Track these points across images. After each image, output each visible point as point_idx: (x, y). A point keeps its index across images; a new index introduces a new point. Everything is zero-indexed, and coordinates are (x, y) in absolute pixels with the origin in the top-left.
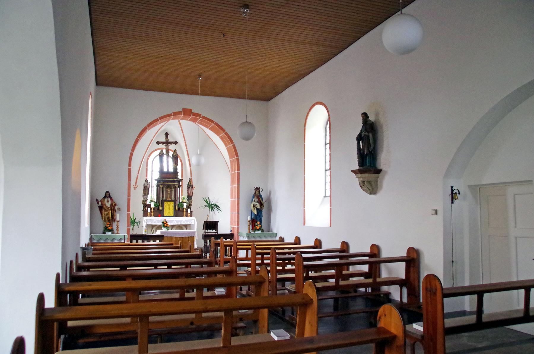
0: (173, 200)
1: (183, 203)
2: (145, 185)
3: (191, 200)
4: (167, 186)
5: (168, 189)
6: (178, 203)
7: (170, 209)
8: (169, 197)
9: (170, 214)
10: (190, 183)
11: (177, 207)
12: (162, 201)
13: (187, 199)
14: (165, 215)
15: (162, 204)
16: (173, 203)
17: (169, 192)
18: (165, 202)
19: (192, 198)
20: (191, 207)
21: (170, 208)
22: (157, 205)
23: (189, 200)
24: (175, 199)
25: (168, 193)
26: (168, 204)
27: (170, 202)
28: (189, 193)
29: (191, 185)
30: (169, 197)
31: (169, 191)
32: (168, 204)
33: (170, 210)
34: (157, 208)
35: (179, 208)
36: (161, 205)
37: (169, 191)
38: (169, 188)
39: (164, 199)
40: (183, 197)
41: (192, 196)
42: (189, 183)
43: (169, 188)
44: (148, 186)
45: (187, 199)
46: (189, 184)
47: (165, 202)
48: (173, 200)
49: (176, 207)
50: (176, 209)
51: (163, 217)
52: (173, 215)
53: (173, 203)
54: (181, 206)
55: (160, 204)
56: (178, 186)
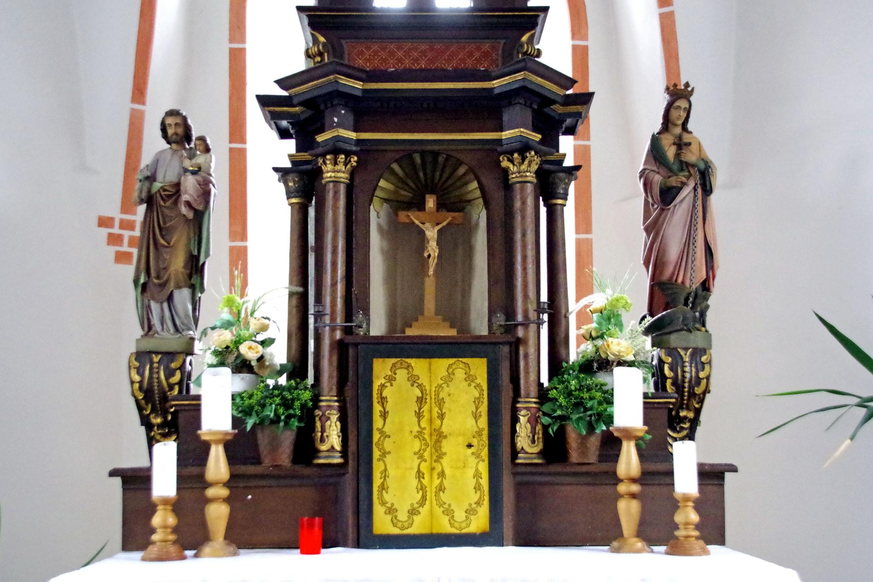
0: (485, 332)
1: (601, 378)
2: (160, 176)
3: (696, 339)
4: (401, 182)
5: (421, 206)
6: (544, 379)
7: (439, 456)
8: (430, 305)
9: (449, 512)
10: (681, 145)
11: (534, 421)
12: (341, 348)
13: (648, 331)
14: (382, 524)
15: (341, 393)
16: (479, 367)
17: (433, 249)
18: (381, 368)
19: (703, 315)
20: (695, 422)
21: (439, 436)
22: (287, 404)
23: (674, 340)
24: (500, 319)
25: (423, 262)
26: (413, 380)
27: (441, 365)
28: (673, 251)
29: (690, 157)
30: (430, 305)
31: (432, 233)
32: (413, 380)
33: (445, 461)
34: (287, 438)
35: (562, 432)
36: (329, 400)
37: (432, 233)
38: (431, 202)
39: (378, 326)
40: (598, 300)
41: (706, 286)
42: (667, 141)
43: (431, 202)
44: (190, 183)
45: (648, 331)
46: (671, 152)
47: (381, 368)
48: (485, 332)
49: (523, 428)
50: (522, 442)
51: (358, 545)
52: (479, 522)
53: (479, 367)
54: (579, 404)
55: (316, 399)
56: (533, 162)
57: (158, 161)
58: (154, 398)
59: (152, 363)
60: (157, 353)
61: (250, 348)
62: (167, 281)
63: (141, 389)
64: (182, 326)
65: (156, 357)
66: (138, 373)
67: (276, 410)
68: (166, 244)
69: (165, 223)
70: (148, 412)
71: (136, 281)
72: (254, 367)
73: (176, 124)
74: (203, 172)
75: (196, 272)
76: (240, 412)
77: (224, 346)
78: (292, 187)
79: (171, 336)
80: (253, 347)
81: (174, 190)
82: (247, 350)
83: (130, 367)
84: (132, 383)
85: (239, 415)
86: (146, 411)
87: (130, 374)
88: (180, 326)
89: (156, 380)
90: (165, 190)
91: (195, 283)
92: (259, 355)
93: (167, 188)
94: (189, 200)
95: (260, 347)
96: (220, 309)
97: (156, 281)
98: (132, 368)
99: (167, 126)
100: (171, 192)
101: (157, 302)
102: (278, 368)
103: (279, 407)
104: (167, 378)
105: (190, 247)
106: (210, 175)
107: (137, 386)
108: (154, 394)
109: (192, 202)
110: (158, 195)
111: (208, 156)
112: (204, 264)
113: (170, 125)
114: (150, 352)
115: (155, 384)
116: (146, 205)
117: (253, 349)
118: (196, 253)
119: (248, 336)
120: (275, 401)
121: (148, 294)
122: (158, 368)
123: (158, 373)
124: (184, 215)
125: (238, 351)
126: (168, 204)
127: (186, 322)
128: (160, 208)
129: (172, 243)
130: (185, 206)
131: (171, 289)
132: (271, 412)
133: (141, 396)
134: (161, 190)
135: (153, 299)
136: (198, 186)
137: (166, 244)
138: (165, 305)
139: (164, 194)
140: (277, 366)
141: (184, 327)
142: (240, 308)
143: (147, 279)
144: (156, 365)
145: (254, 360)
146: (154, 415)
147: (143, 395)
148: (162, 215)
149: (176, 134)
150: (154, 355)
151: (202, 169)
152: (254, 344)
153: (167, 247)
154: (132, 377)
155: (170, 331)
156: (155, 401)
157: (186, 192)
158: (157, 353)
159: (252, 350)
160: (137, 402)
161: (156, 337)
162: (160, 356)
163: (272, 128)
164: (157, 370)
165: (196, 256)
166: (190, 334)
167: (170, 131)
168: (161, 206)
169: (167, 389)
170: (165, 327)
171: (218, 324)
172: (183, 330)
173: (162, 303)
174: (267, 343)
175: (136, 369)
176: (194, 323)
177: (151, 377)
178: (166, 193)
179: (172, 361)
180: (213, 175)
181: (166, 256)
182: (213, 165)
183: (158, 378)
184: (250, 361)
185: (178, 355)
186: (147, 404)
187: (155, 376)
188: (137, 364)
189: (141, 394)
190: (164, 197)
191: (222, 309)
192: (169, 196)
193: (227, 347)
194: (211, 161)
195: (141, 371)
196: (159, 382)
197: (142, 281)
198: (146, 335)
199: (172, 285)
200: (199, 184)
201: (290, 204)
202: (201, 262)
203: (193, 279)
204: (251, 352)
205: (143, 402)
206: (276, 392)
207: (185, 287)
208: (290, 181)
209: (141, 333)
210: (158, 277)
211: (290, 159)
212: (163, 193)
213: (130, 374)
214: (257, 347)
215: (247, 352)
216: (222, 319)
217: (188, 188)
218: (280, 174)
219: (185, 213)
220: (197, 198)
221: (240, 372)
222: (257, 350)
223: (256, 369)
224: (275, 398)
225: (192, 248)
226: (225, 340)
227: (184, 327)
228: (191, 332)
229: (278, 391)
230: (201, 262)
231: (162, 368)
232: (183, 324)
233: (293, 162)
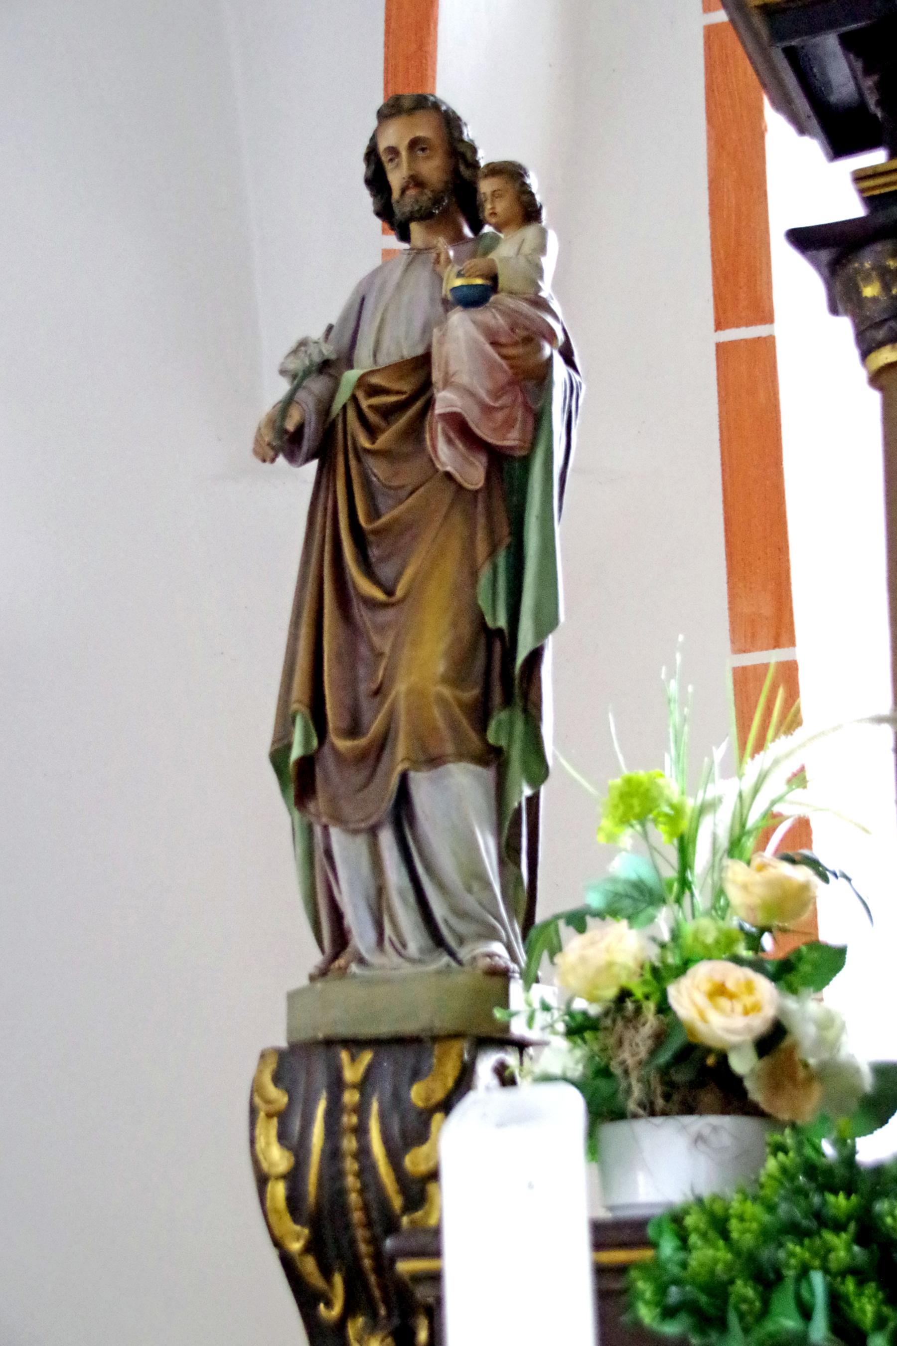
57: (363, 300)
58: (353, 1242)
59: (337, 1085)
60: (355, 1044)
61: (719, 991)
62: (383, 743)
63: (294, 1202)
64: (453, 921)
65: (353, 1059)
66: (282, 1137)
67: (836, 1302)
68: (379, 595)
69: (374, 513)
70: (336, 1311)
71: (279, 758)
72: (749, 1084)
73: (415, 144)
74: (511, 293)
75: (508, 701)
76: (668, 1313)
77: (611, 993)
78: (874, 299)
79: (407, 969)
80: (730, 985)
81: (407, 386)
82: (702, 1000)
83: (253, 1112)
84: (262, 1180)
85: (671, 1329)
86: (329, 1305)
87: (252, 1141)
88: (446, 921)
89: (351, 1165)
90: (374, 391)
91: (503, 743)
92: (759, 1023)
93: (375, 380)
94: (458, 410)
95: (764, 987)
96: (601, 839)
97: (343, 744)
98: (262, 1114)
99: (384, 158)
100: (398, 393)
101: (355, 832)
102: (868, 1082)
103: (850, 1285)
104: (395, 1158)
105: (474, 598)
106: (542, 305)
107: (278, 1191)
108: (348, 1226)
109: (473, 417)
110: (351, 414)
111: (530, 232)
112: (536, 656)
113: (393, 151)
114: (330, 1043)
115: (351, 1181)
116: (314, 464)
117: (731, 996)
118: (502, 622)
119: (717, 942)
120: (829, 1250)
121: (319, 804)
122: (362, 1109)
123: (361, 1131)
124: (448, 476)
125: (664, 1008)
126: (383, 440)
127: (470, 902)
128: (359, 460)
129: (399, 593)
130: (450, 441)
131: (400, 768)
132: (806, 1313)
133: (298, 1239)
134: (360, 395)
135: (339, 820)
136: (489, 348)
137: (379, 595)
138: (387, 838)
139: (370, 407)
140: (857, 1071)
141: (462, 927)
142: (684, 825)
143: (315, 743)
144: (350, 1097)
145: (736, 1047)
146: (361, 1321)
147: (306, 1231)
148: (367, 484)
149: (416, 181)
150: (344, 1056)
151: (502, 282)
152: (735, 976)
153: (385, 605)
154: (261, 1157)
155: (404, 946)
156: (357, 1258)
157: (447, 383)
158: (355, 1044)
159: (724, 1002)
160: (288, 1263)
161: (354, 976)
162: (367, 1057)
163: (802, 130)
164: (354, 1119)
165: (500, 631)
166: (491, 955)
167: (396, 178)
168: (360, 453)
169: (397, 1202)
170: (388, 931)
171: (595, 900)
172: (461, 941)
173: (373, 832)
174: (805, 968)
175: (275, 1121)
176: (512, 910)
177: (333, 1153)
178: (375, 401)
179: (416, 1075)
180: (555, 305)
181: (385, 644)
182: (549, 262)
183: (363, 1153)
184: (723, 1058)
185: (437, 1049)
186: (327, 1274)
187: (349, 1144)
188: (280, 1098)
189: (298, 1228)
190: (372, 417)
191: (612, 837)
192: (389, 413)
193: (624, 995)
194: (542, 249)
195: (296, 1125)
196: (367, 1169)
197: (296, 753)
198: (323, 973)
199: (401, 748)
200: (495, 344)
201: (877, 379)
202: (522, 654)
203: (493, 725)
204: (717, 1007)
205: (309, 1266)
206: (840, 1203)
207: (460, 756)
208: (867, 279)
209: (314, 958)
210: (354, 730)
211: (861, 191)
212: (365, 403)
213: (252, 1141)
214: (750, 987)
215: (704, 1019)
216: (614, 880)
217: (453, 368)
218: (825, 255)
219: (449, 469)
220: (488, 400)
221: (689, 1109)
222: (748, 1000)
223: (756, 1093)
224: (829, 1236)
225: (483, 602)
226: (610, 965)
227: (462, 927)
228: (498, 948)
229: (848, 1196)
230: (522, 654)
231: (375, 1107)
232: (462, 914)
233: (870, 201)
